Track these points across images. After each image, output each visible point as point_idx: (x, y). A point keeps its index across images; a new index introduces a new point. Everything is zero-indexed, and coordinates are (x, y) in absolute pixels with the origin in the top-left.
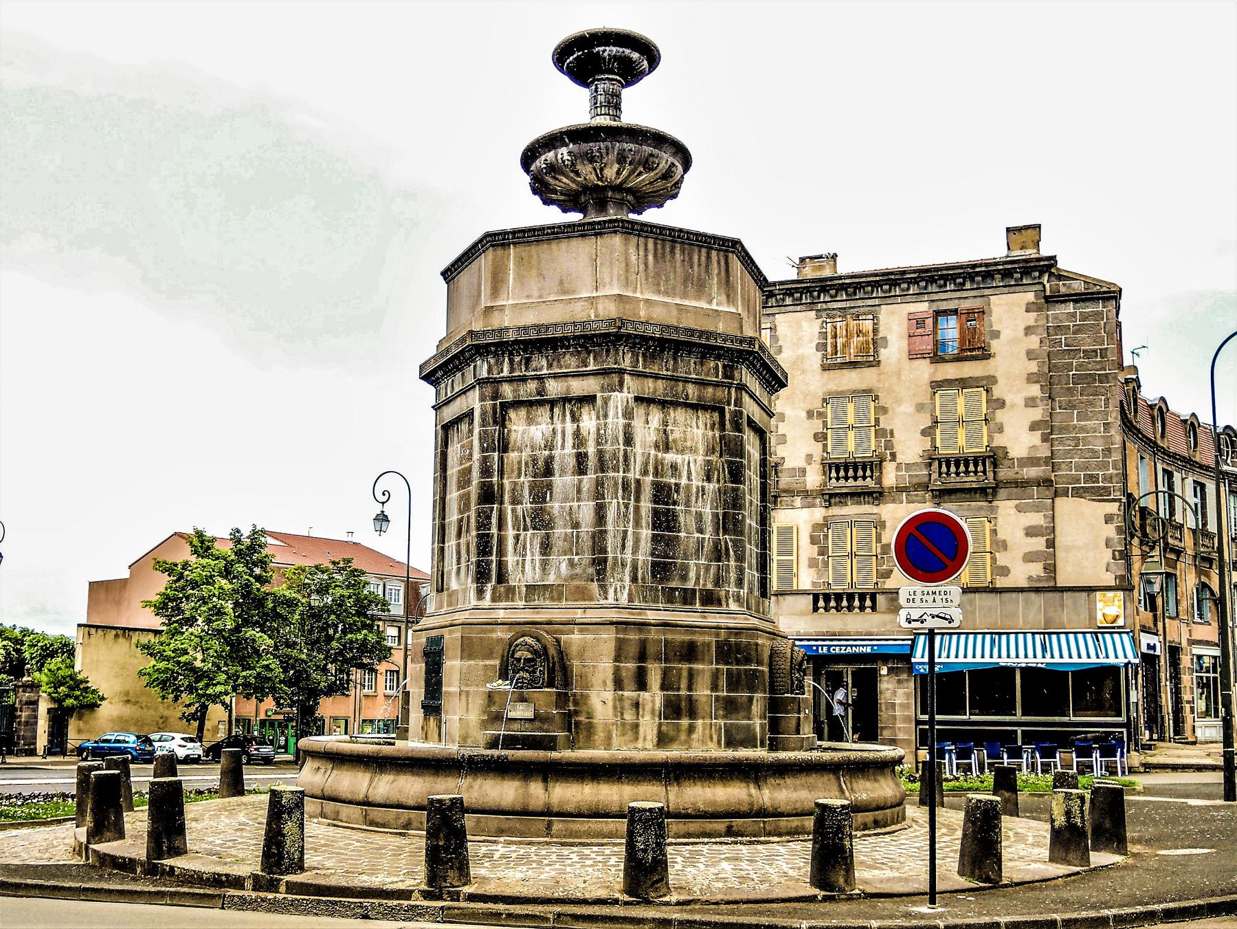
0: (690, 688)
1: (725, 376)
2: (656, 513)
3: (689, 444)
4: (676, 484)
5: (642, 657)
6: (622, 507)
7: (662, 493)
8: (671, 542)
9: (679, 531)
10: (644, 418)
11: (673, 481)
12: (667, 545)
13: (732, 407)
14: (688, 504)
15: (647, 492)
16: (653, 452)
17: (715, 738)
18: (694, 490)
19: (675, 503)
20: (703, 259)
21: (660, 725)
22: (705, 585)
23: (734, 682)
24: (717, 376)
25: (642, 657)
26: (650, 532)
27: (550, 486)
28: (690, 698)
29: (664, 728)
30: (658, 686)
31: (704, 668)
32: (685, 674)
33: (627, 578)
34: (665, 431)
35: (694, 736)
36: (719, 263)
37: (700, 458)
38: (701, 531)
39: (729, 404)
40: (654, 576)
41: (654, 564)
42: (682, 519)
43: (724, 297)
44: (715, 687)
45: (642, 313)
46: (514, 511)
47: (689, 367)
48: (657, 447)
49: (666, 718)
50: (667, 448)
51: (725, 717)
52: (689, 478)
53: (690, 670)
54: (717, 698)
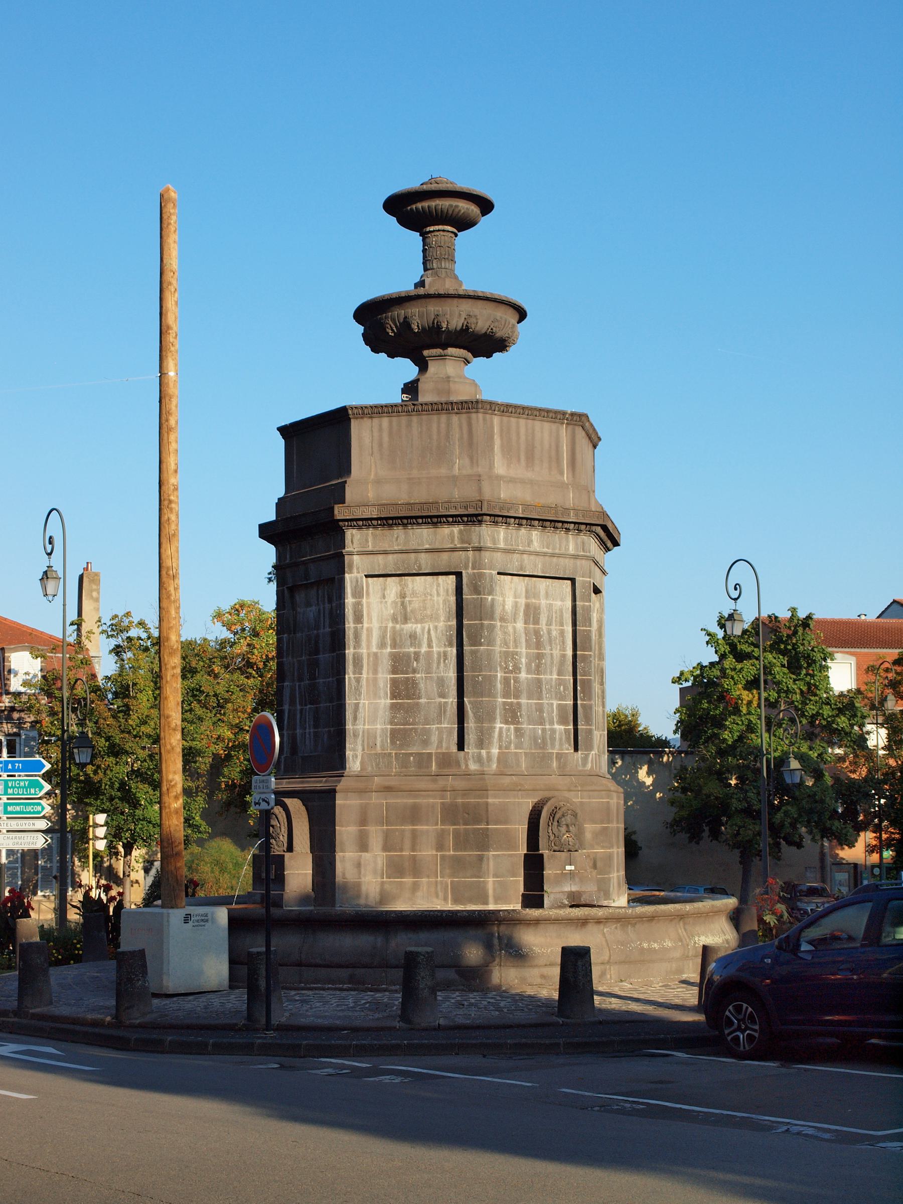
1: (462, 541)
2: (394, 683)
4: (415, 653)
5: (363, 822)
6: (353, 681)
7: (399, 663)
8: (411, 710)
9: (419, 698)
10: (380, 595)
11: (412, 650)
12: (407, 712)
13: (470, 571)
14: (428, 671)
15: (385, 663)
16: (390, 625)
17: (441, 894)
18: (436, 655)
19: (414, 671)
20: (443, 426)
21: (383, 883)
22: (447, 748)
23: (461, 842)
24: (453, 541)
25: (363, 822)
26: (389, 701)
28: (414, 859)
29: (387, 887)
31: (429, 829)
32: (408, 835)
33: (360, 748)
34: (403, 603)
35: (419, 894)
36: (461, 427)
37: (441, 625)
38: (443, 695)
39: (466, 568)
40: (393, 742)
41: (394, 733)
42: (422, 686)
43: (467, 461)
44: (440, 847)
45: (370, 495)
46: (299, 686)
47: (423, 535)
48: (395, 619)
50: (406, 620)
51: (450, 877)
52: (430, 645)
53: (414, 834)
54: (443, 857)
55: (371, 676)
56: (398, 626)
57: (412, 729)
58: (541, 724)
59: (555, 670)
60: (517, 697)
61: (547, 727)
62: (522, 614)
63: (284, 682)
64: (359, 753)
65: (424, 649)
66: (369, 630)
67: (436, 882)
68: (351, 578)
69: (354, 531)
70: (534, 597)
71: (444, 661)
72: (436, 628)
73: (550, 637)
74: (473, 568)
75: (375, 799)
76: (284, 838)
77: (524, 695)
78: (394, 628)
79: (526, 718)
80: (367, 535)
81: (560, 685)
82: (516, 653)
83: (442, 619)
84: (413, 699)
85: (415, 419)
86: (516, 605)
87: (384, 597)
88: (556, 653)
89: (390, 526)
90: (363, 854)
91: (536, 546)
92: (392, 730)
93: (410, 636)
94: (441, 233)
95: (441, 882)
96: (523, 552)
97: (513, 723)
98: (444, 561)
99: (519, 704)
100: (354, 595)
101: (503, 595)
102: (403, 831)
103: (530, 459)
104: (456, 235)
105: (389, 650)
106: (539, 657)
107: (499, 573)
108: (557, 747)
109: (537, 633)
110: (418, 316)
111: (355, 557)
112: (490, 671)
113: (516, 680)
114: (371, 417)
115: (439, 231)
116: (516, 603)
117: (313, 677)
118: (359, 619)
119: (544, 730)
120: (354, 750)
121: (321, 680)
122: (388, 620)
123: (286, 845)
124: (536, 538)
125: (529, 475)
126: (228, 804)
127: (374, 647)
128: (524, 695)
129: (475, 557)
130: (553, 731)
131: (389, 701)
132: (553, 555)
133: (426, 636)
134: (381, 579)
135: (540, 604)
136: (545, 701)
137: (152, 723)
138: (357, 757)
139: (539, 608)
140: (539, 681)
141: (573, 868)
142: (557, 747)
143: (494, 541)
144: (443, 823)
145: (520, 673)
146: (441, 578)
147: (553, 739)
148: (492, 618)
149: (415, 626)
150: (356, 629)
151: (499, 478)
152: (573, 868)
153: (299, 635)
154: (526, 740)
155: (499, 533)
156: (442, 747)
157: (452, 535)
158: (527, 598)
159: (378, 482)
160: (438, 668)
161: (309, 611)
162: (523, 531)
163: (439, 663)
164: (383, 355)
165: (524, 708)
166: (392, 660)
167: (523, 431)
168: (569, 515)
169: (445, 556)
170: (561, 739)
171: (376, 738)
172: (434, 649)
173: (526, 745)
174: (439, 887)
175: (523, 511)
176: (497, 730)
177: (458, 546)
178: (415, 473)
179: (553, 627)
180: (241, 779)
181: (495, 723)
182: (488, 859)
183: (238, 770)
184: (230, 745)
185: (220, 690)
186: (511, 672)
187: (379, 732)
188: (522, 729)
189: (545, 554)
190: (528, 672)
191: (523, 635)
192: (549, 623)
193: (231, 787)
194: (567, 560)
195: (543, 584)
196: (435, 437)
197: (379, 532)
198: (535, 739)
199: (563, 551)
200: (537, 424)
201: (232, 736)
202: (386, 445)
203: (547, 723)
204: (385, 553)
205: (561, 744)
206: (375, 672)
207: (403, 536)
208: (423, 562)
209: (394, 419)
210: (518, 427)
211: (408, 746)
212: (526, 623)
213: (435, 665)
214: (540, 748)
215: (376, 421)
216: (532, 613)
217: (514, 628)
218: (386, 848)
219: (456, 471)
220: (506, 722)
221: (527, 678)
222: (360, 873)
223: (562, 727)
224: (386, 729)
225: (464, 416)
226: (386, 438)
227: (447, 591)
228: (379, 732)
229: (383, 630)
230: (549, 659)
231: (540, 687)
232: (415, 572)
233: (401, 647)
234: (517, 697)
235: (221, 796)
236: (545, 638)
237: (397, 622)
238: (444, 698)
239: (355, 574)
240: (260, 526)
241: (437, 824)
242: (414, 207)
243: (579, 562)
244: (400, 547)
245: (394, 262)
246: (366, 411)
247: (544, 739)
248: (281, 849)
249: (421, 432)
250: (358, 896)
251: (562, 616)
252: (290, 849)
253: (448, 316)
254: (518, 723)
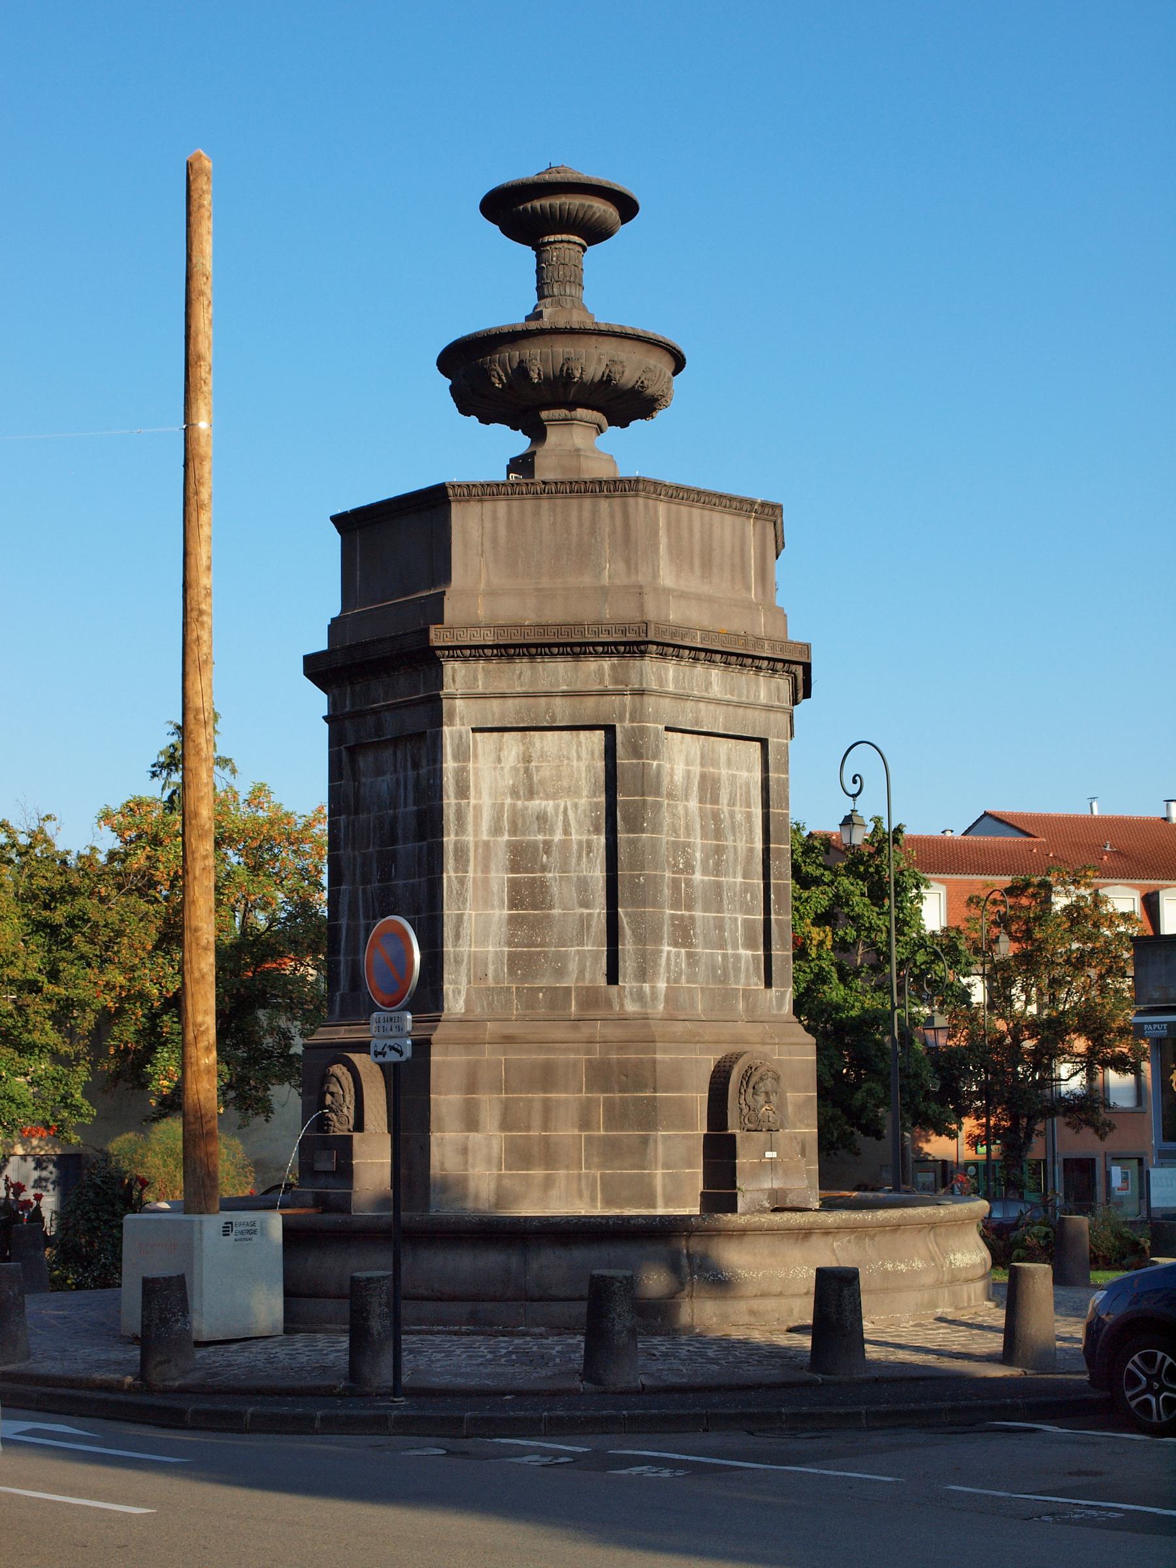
0: (545, 1127)
1: (616, 681)
2: (514, 885)
3: (565, 783)
4: (545, 842)
5: (471, 1086)
7: (522, 857)
8: (539, 925)
9: (551, 907)
10: (493, 756)
11: (540, 837)
12: (532, 928)
13: (627, 724)
14: (564, 869)
15: (501, 857)
16: (508, 801)
17: (586, 1193)
18: (575, 847)
19: (544, 869)
20: (586, 514)
22: (593, 980)
23: (616, 1116)
24: (601, 681)
25: (471, 1086)
26: (506, 912)
27: (393, 857)
28: (546, 1141)
29: (506, 1182)
30: (496, 1123)
31: (568, 1098)
32: (538, 1106)
33: (464, 980)
34: (527, 770)
35: (554, 1192)
36: (612, 517)
37: (583, 801)
38: (585, 904)
39: (622, 720)
40: (512, 972)
42: (555, 890)
43: (621, 565)
44: (585, 1124)
45: (481, 612)
47: (558, 672)
48: (515, 793)
49: (508, 1168)
50: (531, 794)
52: (566, 832)
53: (546, 1103)
54: (589, 1139)
55: (480, 875)
56: (519, 803)
57: (539, 953)
58: (721, 948)
59: (739, 869)
60: (689, 907)
61: (730, 952)
62: (695, 788)
63: (340, 885)
64: (463, 987)
65: (558, 837)
66: (478, 809)
67: (580, 1175)
68: (451, 733)
69: (457, 665)
70: (712, 765)
71: (588, 854)
72: (576, 806)
73: (733, 823)
74: (632, 720)
75: (489, 1054)
76: (349, 1111)
77: (699, 905)
78: (514, 806)
79: (701, 938)
80: (476, 670)
81: (746, 891)
82: (689, 845)
83: (585, 793)
84: (542, 909)
85: (545, 504)
86: (688, 775)
87: (499, 760)
88: (742, 845)
89: (511, 658)
90: (471, 1134)
91: (716, 691)
92: (510, 954)
93: (537, 818)
94: (564, 245)
95: (587, 1175)
96: (699, 699)
97: (685, 947)
98: (589, 709)
99: (692, 918)
100: (456, 758)
101: (671, 760)
102: (531, 1100)
103: (707, 565)
104: (585, 250)
105: (506, 837)
106: (719, 850)
107: (667, 729)
108: (742, 980)
109: (716, 816)
110: (540, 359)
111: (458, 702)
112: (656, 869)
113: (689, 883)
114: (481, 501)
115: (562, 241)
116: (688, 772)
117: (386, 877)
118: (463, 791)
119: (725, 956)
120: (455, 982)
121: (401, 882)
122: (504, 794)
123: (352, 1121)
124: (715, 680)
125: (706, 589)
126: (117, 1076)
127: (485, 833)
128: (699, 905)
129: (634, 704)
130: (737, 958)
131: (506, 912)
132: (739, 705)
133: (561, 817)
134: (495, 734)
135: (720, 774)
136: (726, 915)
137: (20, 963)
138: (459, 992)
139: (719, 780)
140: (719, 885)
141: (774, 1154)
142: (742, 980)
143: (661, 681)
144: (589, 1090)
145: (693, 873)
146: (583, 735)
147: (737, 970)
148: (657, 793)
149: (544, 803)
150: (459, 806)
151: (667, 591)
152: (774, 1154)
153: (363, 816)
154: (701, 970)
155: (667, 670)
156: (584, 979)
157: (600, 671)
158: (702, 765)
159: (492, 593)
160: (578, 864)
161: (381, 780)
162: (699, 669)
163: (580, 857)
164: (474, 418)
165: (698, 923)
166: (511, 852)
167: (697, 525)
168: (763, 647)
169: (590, 702)
170: (747, 970)
171: (486, 965)
172: (573, 837)
173: (701, 977)
174: (583, 1182)
175: (703, 639)
176: (665, 954)
177: (610, 687)
178: (545, 582)
179: (737, 809)
180: (137, 1042)
181: (661, 944)
182: (656, 1142)
183: (132, 1029)
184: (124, 994)
185: (113, 917)
186: (682, 871)
187: (491, 957)
188: (696, 954)
189: (728, 703)
190: (705, 872)
191: (698, 819)
192: (732, 803)
193: (123, 1053)
194: (757, 713)
195: (724, 745)
196: (574, 531)
197: (493, 666)
198: (714, 969)
199: (752, 700)
200: (716, 517)
201: (124, 982)
202: (502, 541)
203: (729, 946)
204: (503, 696)
205: (748, 977)
206: (486, 869)
207: (529, 673)
208: (558, 712)
209: (515, 503)
210: (690, 520)
211: (535, 977)
212: (701, 802)
213: (574, 861)
214: (721, 982)
215: (488, 506)
216: (709, 788)
217: (686, 808)
218: (505, 1125)
219: (605, 580)
220: (675, 944)
221: (703, 881)
222: (466, 1163)
223: (750, 953)
224: (502, 952)
225: (617, 501)
226: (502, 532)
227: (593, 753)
228: (491, 957)
229: (498, 810)
230: (731, 855)
231: (720, 895)
232: (545, 724)
233: (524, 834)
234: (689, 907)
235: (108, 1066)
236: (726, 824)
237: (518, 798)
238: (587, 907)
239: (457, 727)
240: (305, 657)
241: (580, 1091)
242: (529, 205)
243: (772, 716)
244: (524, 689)
245: (498, 286)
246: (474, 491)
247: (725, 969)
248: (345, 1127)
249: (554, 524)
250: (464, 1197)
251: (748, 792)
252: (359, 1126)
253: (583, 361)
254: (691, 945)
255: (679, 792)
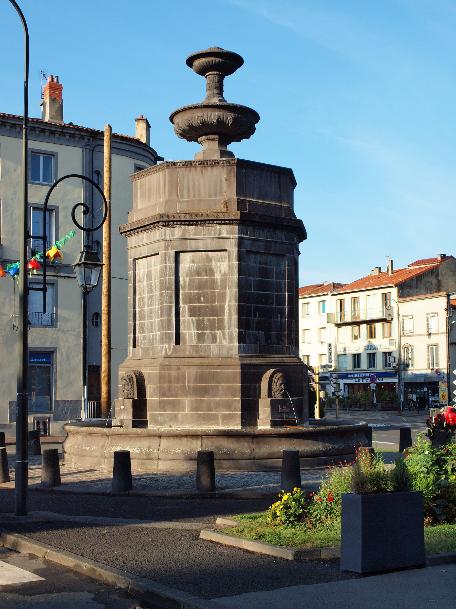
58: (152, 332)
60: (144, 320)
97: (142, 333)
99: (144, 323)
109: (151, 285)
113: (144, 310)
116: (144, 271)
119: (153, 335)
128: (146, 318)
130: (156, 335)
147: (156, 340)
165: (146, 325)
173: (147, 344)
190: (148, 306)
217: (143, 285)
230: (155, 298)
231: (151, 313)
247: (153, 339)
255: (142, 280)
